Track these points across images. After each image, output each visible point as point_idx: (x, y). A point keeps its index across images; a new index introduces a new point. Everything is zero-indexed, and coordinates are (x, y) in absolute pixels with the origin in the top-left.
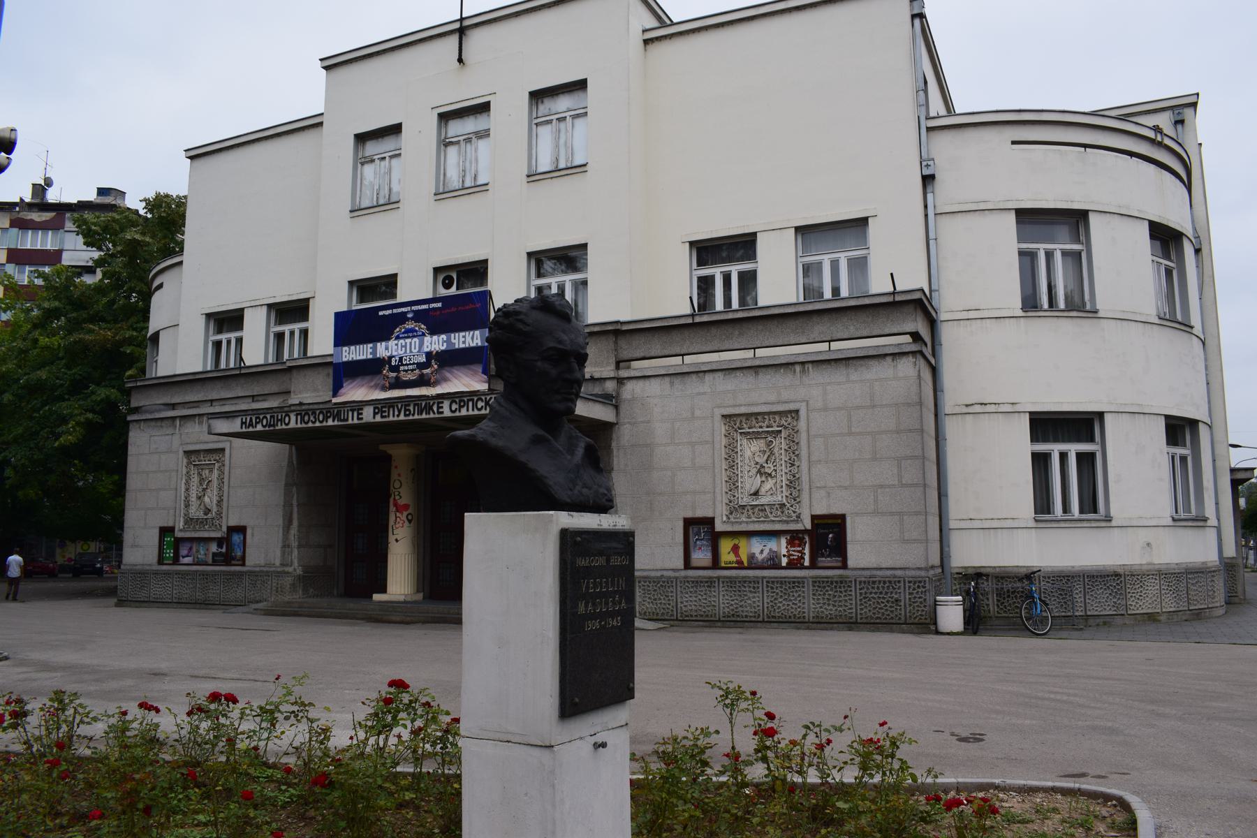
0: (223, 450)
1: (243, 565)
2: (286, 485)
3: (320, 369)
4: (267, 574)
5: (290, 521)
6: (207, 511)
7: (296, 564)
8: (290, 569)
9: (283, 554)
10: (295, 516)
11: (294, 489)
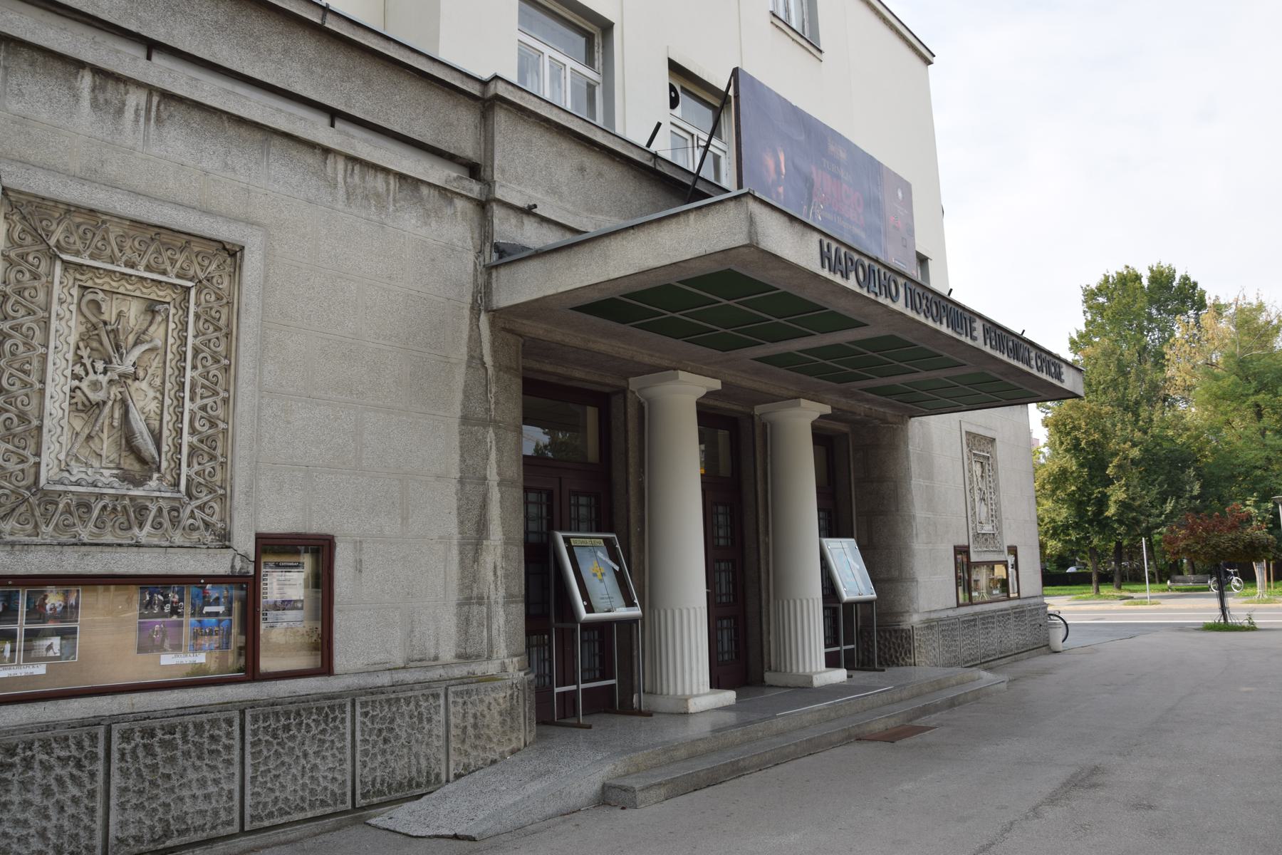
0: (233, 253)
1: (326, 668)
2: (465, 420)
3: (565, 145)
4: (430, 690)
5: (482, 528)
6: (141, 463)
7: (502, 650)
8: (492, 668)
9: (465, 623)
10: (495, 512)
11: (491, 435)
